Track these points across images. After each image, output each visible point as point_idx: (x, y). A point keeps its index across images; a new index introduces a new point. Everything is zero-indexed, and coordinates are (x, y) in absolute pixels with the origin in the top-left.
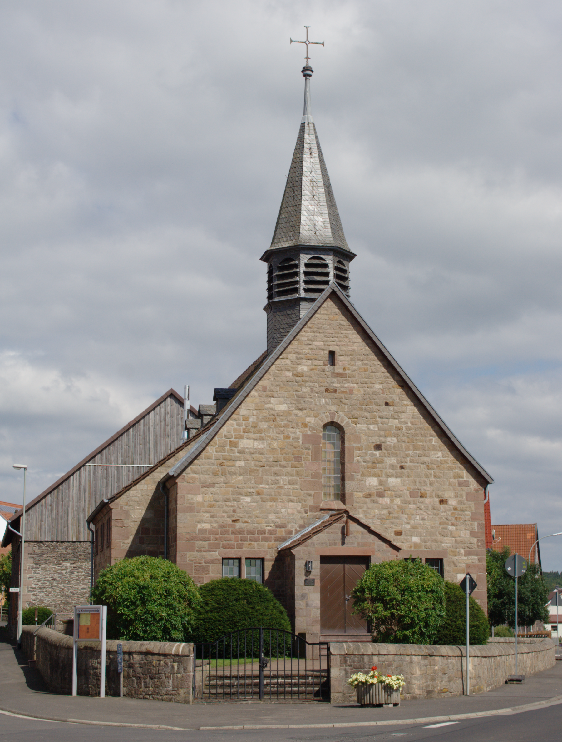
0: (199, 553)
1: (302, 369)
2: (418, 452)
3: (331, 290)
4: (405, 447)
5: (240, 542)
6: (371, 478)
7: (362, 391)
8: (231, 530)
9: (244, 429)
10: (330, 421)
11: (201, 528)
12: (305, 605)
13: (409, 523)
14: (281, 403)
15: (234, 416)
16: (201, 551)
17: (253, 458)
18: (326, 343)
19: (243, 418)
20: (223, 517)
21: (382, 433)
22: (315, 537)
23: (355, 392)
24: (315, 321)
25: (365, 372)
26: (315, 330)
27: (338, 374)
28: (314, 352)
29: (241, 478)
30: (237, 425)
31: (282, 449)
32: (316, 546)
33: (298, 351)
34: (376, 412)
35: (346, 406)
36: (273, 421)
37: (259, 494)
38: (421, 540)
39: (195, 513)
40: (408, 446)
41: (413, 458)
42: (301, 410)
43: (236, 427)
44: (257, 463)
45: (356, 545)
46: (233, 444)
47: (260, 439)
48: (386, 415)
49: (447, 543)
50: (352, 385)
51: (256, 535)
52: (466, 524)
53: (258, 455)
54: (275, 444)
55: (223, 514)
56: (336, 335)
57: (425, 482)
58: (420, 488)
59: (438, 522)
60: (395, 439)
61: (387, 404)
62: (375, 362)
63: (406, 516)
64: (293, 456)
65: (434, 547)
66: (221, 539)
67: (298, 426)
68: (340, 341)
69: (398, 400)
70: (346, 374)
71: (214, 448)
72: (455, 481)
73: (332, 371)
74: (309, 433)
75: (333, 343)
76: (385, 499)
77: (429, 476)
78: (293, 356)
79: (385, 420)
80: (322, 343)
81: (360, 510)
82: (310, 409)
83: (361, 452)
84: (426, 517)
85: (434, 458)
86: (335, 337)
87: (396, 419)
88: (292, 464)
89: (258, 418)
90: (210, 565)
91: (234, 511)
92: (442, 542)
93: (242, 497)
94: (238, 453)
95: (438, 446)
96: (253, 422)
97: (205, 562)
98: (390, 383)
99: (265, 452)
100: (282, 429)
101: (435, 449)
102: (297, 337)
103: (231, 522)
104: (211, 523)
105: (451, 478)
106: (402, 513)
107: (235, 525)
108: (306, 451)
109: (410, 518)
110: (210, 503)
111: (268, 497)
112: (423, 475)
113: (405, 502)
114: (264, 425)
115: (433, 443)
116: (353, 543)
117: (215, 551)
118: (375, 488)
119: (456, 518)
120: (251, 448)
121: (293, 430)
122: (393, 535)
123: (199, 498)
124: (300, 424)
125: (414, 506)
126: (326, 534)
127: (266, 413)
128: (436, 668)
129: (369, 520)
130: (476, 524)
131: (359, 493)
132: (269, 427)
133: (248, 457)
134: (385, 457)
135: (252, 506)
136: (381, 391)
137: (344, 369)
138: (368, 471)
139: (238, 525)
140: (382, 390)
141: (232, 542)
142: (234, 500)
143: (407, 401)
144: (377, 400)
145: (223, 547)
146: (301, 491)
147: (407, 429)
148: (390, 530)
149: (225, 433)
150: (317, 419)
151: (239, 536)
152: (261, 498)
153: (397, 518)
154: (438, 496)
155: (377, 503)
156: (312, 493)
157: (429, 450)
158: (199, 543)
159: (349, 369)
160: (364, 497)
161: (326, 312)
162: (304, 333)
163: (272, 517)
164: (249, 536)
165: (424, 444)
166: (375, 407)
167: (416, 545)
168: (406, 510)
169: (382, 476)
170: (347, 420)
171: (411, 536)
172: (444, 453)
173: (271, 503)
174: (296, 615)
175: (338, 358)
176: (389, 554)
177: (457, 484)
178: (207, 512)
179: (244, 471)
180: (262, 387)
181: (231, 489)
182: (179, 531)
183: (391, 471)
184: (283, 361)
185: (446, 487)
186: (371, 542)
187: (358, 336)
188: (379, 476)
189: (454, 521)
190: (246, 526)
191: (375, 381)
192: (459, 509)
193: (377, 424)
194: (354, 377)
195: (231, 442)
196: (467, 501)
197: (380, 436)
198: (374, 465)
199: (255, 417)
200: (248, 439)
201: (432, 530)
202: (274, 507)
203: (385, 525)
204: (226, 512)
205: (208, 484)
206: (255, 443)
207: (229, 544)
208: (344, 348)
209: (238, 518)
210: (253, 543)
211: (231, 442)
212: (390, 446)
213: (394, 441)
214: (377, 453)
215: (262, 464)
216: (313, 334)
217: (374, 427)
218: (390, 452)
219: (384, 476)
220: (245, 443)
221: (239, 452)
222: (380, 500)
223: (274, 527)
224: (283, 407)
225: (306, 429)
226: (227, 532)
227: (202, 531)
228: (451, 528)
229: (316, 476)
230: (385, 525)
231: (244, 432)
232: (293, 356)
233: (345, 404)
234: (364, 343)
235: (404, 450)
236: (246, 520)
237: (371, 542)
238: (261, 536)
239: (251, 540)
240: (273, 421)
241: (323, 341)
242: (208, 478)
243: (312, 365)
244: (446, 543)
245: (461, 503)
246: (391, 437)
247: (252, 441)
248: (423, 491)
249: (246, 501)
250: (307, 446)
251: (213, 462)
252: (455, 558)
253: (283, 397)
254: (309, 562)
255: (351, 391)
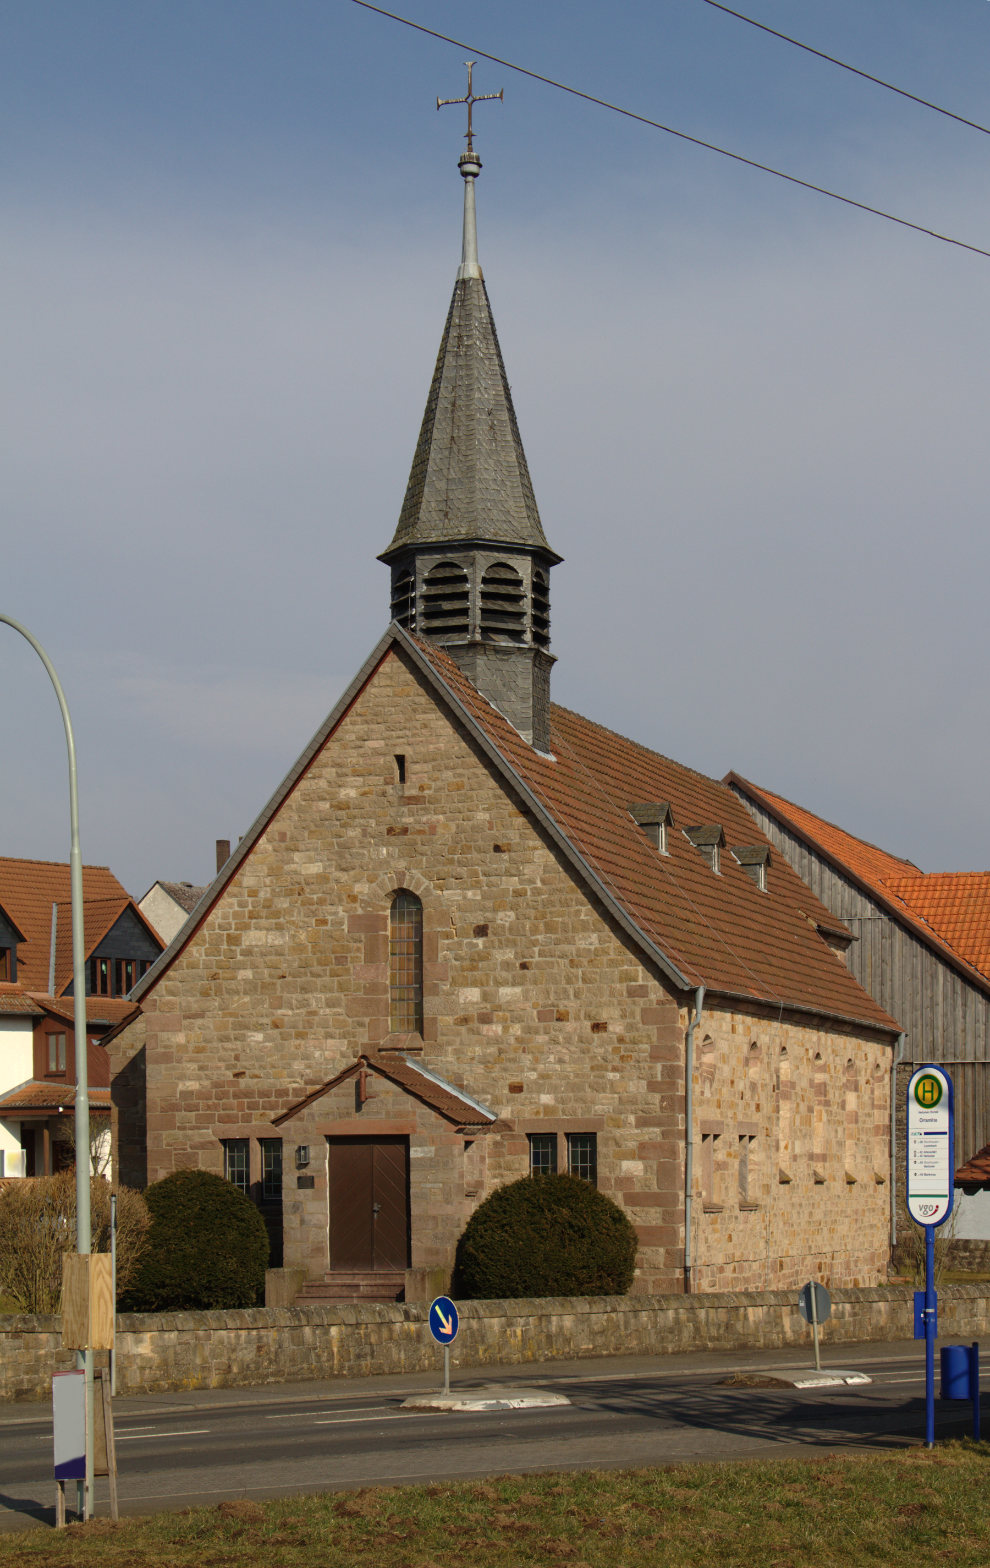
0: (181, 1132)
1: (346, 795)
2: (553, 936)
3: (391, 640)
4: (530, 928)
5: (247, 1111)
6: (469, 989)
7: (453, 828)
8: (231, 1090)
9: (250, 912)
10: (396, 887)
11: (184, 1088)
12: (298, 1222)
13: (534, 1070)
14: (311, 861)
15: (230, 889)
16: (184, 1128)
17: (265, 962)
18: (391, 742)
19: (249, 892)
20: (219, 1068)
21: (489, 904)
22: (314, 1103)
23: (440, 830)
24: (369, 701)
25: (459, 789)
26: (369, 718)
27: (409, 798)
28: (368, 761)
29: (247, 999)
30: (239, 906)
31: (315, 945)
32: (317, 1119)
33: (339, 761)
34: (478, 865)
35: (424, 858)
36: (299, 894)
37: (276, 1026)
38: (556, 1099)
39: (174, 1064)
40: (534, 925)
41: (546, 948)
42: (345, 870)
43: (237, 908)
44: (273, 971)
45: (383, 1116)
46: (233, 940)
47: (277, 929)
48: (496, 869)
49: (603, 1104)
50: (434, 818)
51: (273, 1099)
52: (639, 1068)
53: (274, 958)
54: (303, 936)
55: (220, 1064)
56: (408, 725)
57: (565, 991)
58: (556, 1002)
59: (588, 1066)
60: (512, 914)
61: (497, 849)
62: (476, 771)
63: (530, 1057)
64: (333, 956)
65: (579, 1112)
66: (216, 1107)
67: (340, 900)
68: (413, 736)
69: (517, 840)
70: (424, 797)
71: (203, 949)
72: (621, 987)
73: (400, 793)
74: (360, 911)
75: (401, 740)
76: (494, 1027)
77: (574, 979)
78: (330, 773)
79: (493, 879)
80: (382, 743)
81: (450, 1049)
82: (362, 867)
83: (450, 941)
84: (567, 1058)
85: (583, 946)
86: (405, 728)
87: (515, 876)
88: (331, 970)
89: (273, 890)
90: (200, 1152)
91: (237, 1058)
92: (593, 1102)
93: (249, 1034)
94: (241, 955)
95: (591, 922)
96: (265, 900)
97: (191, 1148)
98: (504, 807)
99: (286, 952)
100: (313, 908)
101: (585, 927)
102: (337, 734)
103: (231, 1078)
104: (199, 1079)
105: (613, 982)
106: (524, 1051)
107: (238, 1082)
108: (355, 945)
109: (536, 1060)
110: (197, 1045)
111: (293, 1031)
112: (563, 979)
113: (528, 1030)
114: (283, 903)
115: (582, 917)
116: (378, 1113)
117: (207, 1128)
118: (476, 1007)
119: (622, 1058)
120: (262, 945)
121: (333, 909)
122: (506, 1091)
123: (180, 1038)
124: (344, 897)
125: (546, 1037)
126: (334, 1098)
127: (286, 881)
128: (42, 1352)
129: (464, 1066)
130: (659, 1067)
131: (447, 1018)
132: (292, 904)
133: (259, 960)
134: (494, 948)
135: (266, 1047)
136: (487, 825)
137: (422, 788)
138: (463, 976)
139: (243, 1082)
140: (489, 822)
141: (235, 1112)
142: (236, 1039)
143: (535, 841)
144: (480, 843)
145: (219, 1121)
146: (348, 1019)
147: (533, 894)
148: (501, 1083)
149: (220, 920)
150: (374, 885)
151: (246, 1100)
152: (281, 1034)
153: (513, 1060)
154: (588, 1017)
155: (479, 1034)
156: (367, 1020)
157: (575, 930)
158: (180, 1115)
159: (430, 788)
160: (455, 1024)
161: (388, 682)
162: (350, 727)
163: (298, 1066)
164: (261, 1100)
165: (566, 919)
166: (475, 856)
167: (548, 1109)
168: (530, 1045)
169: (488, 984)
170: (427, 882)
171: (539, 1092)
172: (602, 934)
173: (298, 1042)
174: (285, 1239)
175: (410, 767)
176: (442, 1130)
177: (625, 993)
178: (193, 1061)
179: (252, 987)
180: (280, 834)
181: (231, 1020)
182: (150, 1095)
183: (504, 974)
184: (313, 782)
185: (605, 999)
186: (410, 1109)
187: (448, 723)
188: (482, 985)
189: (617, 1062)
190: (257, 1084)
191: (477, 806)
192: (628, 1040)
193: (480, 888)
194: (437, 801)
195: (228, 935)
196: (644, 1023)
197: (484, 909)
198: (475, 964)
199: (268, 889)
200: (256, 929)
201: (577, 1080)
202: (302, 1048)
203: (494, 1075)
204: (224, 1061)
205: (193, 1012)
206: (270, 937)
207: (228, 1116)
208: (422, 749)
209: (242, 1070)
210: (267, 1112)
211: (228, 935)
212: (503, 927)
213: (509, 917)
214: (480, 942)
215: (281, 974)
216: (365, 727)
217: (474, 895)
218: (503, 938)
219: (491, 983)
220: (253, 938)
221: (244, 953)
222: (485, 1028)
223: (302, 1082)
224: (315, 869)
225: (354, 905)
226: (225, 1095)
227: (186, 1094)
228: (611, 1075)
229: (373, 988)
230: (494, 1075)
231: (250, 918)
232: (330, 773)
233: (422, 854)
234: (457, 735)
235: (528, 933)
236: (256, 1072)
237: (410, 1109)
238: (280, 1100)
239: (264, 1108)
240: (299, 894)
241: (383, 739)
242: (194, 1002)
243: (364, 785)
244: (602, 1104)
245: (630, 1027)
246: (505, 910)
247: (265, 932)
248: (561, 1008)
249: (255, 1039)
250: (356, 935)
251: (201, 974)
252: (618, 1133)
253: (316, 849)
254: (304, 1148)
255: (433, 829)
